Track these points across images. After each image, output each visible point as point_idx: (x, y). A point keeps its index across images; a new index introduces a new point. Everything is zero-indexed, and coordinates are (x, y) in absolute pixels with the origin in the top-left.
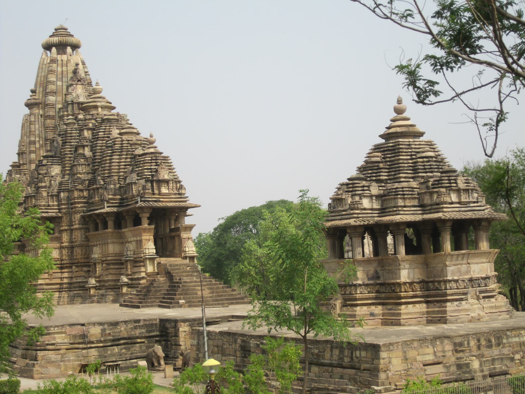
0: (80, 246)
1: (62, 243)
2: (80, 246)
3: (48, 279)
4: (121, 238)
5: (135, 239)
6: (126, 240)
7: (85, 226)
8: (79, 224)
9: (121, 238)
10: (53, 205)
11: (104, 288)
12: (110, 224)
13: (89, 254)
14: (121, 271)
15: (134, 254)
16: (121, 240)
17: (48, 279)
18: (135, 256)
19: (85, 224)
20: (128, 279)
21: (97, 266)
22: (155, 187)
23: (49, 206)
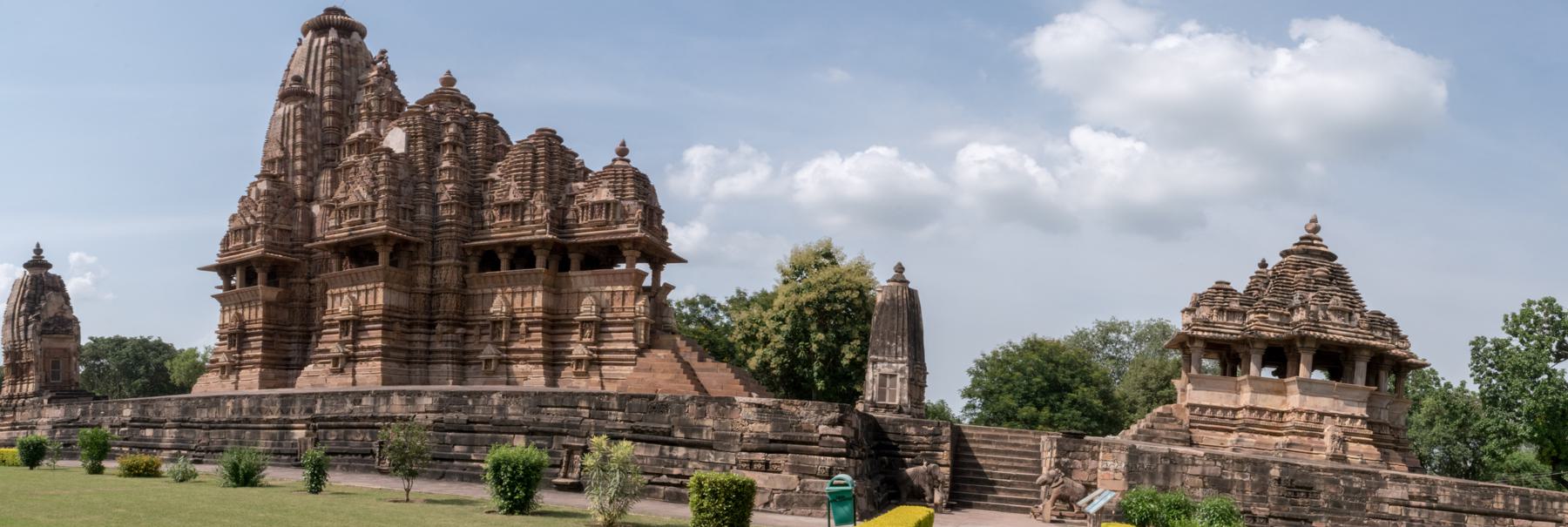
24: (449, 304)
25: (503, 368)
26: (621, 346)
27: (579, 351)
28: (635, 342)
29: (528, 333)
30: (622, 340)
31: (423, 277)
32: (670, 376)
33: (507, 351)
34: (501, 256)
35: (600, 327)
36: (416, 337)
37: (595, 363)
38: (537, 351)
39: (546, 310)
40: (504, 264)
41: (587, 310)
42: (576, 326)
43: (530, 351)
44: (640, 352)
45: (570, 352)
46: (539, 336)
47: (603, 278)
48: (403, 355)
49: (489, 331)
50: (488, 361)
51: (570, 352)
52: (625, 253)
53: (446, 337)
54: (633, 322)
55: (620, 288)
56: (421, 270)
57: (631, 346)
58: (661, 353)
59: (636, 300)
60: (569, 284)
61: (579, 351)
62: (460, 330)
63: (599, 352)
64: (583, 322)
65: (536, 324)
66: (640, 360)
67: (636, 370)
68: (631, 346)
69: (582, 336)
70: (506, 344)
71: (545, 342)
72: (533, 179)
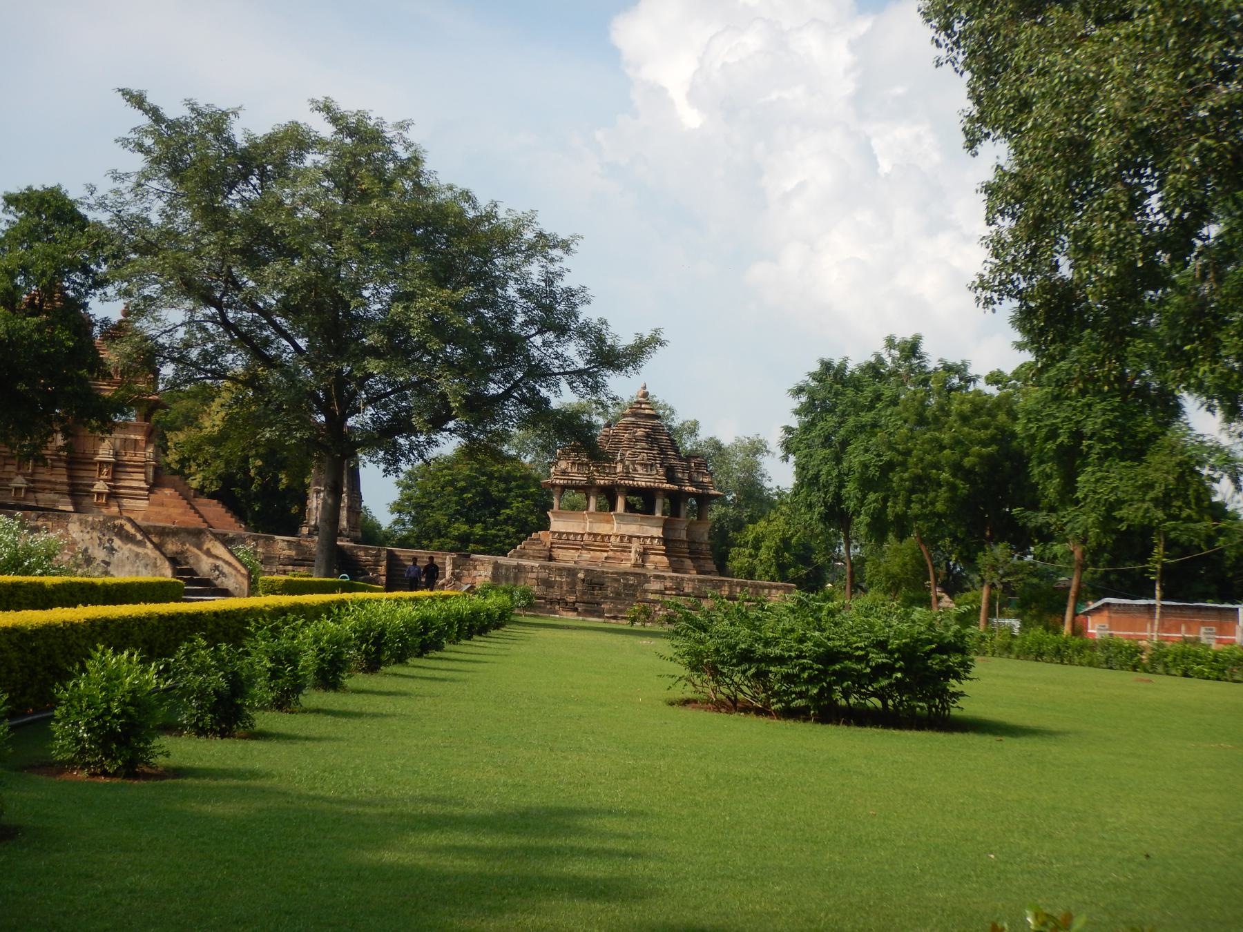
25: (31, 496)
27: (100, 486)
30: (136, 480)
32: (181, 510)
33: (33, 481)
35: (117, 467)
37: (113, 495)
41: (104, 452)
42: (95, 464)
43: (56, 483)
44: (151, 490)
49: (16, 462)
50: (18, 489)
51: (93, 486)
54: (144, 466)
57: (143, 485)
58: (168, 491)
61: (100, 486)
63: (115, 487)
64: (101, 463)
65: (60, 460)
66: (152, 496)
67: (150, 504)
68: (143, 485)
69: (100, 473)
70: (32, 475)
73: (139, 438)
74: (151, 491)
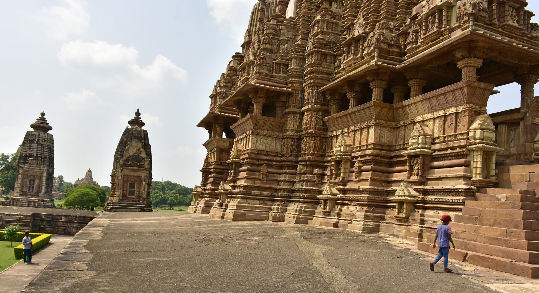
0: (312, 135)
1: (287, 131)
2: (312, 135)
3: (260, 180)
4: (394, 119)
5: (441, 113)
6: (410, 120)
7: (323, 107)
8: (316, 103)
9: (394, 119)
10: (279, 77)
11: (354, 203)
12: (376, 94)
13: (325, 150)
14: (388, 177)
15: (433, 144)
16: (393, 124)
17: (260, 180)
18: (435, 147)
19: (324, 105)
20: (416, 190)
21: (342, 165)
22: (495, 12)
23: (273, 77)
24: (308, 144)
26: (448, 185)
27: (402, 191)
28: (467, 178)
29: (361, 171)
31: (291, 124)
32: (497, 232)
33: (344, 192)
34: (348, 96)
36: (282, 178)
38: (365, 191)
39: (377, 145)
40: (351, 102)
45: (393, 192)
46: (367, 175)
47: (434, 102)
48: (269, 193)
51: (393, 192)
52: (460, 64)
53: (305, 177)
55: (453, 110)
56: (290, 117)
59: (471, 122)
60: (406, 116)
62: (316, 171)
63: (425, 192)
64: (412, 157)
68: (461, 185)
71: (373, 181)
72: (377, 11)
73: (460, 109)
74: (470, 194)
